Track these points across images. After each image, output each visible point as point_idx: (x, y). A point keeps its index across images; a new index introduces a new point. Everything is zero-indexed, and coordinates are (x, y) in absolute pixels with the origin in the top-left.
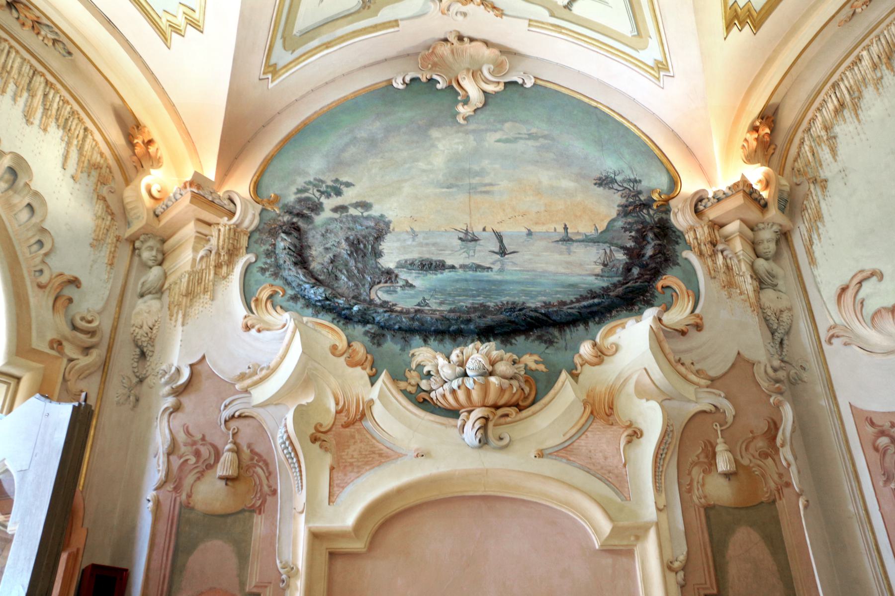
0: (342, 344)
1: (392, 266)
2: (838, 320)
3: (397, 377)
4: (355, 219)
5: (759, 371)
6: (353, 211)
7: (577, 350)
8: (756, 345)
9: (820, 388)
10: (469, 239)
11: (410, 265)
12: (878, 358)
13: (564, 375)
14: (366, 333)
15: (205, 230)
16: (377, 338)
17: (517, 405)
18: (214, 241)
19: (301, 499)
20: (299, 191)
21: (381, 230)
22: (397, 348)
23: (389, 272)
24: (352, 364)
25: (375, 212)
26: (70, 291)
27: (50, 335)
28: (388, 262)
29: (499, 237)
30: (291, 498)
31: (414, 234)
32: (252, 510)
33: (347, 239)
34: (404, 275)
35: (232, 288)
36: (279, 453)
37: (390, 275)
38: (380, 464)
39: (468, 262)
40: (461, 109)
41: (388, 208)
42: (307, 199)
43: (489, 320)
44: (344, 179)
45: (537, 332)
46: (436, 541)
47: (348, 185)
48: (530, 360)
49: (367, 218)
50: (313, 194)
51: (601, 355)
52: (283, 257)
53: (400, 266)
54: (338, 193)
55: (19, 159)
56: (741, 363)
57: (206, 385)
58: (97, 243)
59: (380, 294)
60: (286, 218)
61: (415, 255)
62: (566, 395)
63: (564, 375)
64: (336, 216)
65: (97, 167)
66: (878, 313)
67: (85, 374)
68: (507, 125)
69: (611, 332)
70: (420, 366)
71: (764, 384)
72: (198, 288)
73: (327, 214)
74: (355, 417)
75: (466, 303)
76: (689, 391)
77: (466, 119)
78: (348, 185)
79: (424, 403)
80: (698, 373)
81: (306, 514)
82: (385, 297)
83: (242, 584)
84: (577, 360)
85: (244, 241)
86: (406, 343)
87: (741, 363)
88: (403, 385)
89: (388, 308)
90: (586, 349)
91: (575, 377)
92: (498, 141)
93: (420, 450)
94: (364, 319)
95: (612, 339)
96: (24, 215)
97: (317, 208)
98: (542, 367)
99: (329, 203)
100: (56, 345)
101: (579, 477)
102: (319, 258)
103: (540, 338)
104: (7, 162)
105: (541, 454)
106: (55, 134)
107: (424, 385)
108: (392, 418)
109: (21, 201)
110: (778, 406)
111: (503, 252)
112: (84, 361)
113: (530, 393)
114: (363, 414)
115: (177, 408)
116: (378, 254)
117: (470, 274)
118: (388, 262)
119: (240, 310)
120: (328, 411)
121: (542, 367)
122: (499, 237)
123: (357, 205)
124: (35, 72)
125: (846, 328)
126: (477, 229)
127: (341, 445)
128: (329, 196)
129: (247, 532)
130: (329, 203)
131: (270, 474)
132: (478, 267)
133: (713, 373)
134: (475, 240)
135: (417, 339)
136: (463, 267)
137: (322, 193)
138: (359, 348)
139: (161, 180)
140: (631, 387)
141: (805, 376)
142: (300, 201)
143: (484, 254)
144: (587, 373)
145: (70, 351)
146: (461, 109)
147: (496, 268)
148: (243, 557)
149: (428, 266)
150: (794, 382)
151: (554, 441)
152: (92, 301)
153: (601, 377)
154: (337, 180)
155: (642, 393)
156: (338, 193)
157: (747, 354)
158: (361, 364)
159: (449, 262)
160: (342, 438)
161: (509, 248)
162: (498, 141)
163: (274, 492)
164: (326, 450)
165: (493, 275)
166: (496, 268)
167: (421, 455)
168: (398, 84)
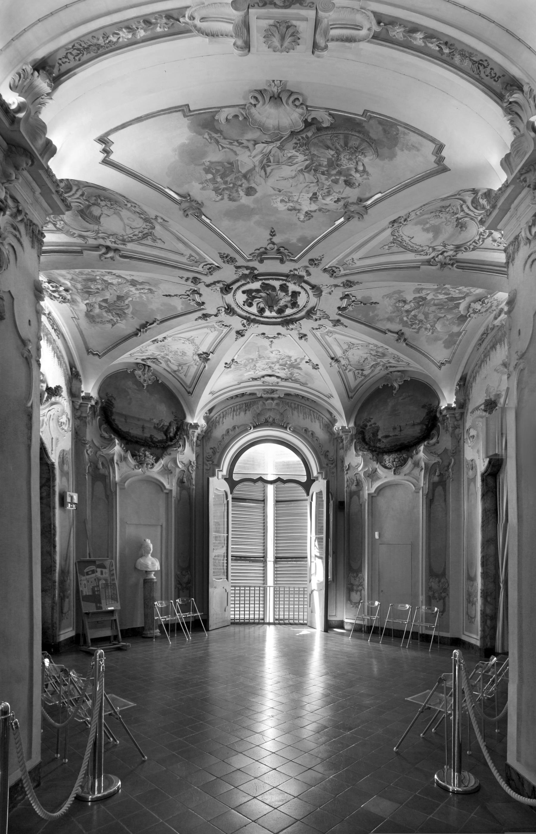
0: (372, 457)
6: (373, 426)
10: (395, 428)
16: (378, 454)
25: (377, 425)
26: (327, 454)
27: (326, 463)
28: (379, 437)
29: (400, 427)
35: (353, 448)
37: (380, 440)
41: (380, 424)
43: (397, 447)
46: (388, 493)
53: (382, 437)
54: (370, 421)
55: (312, 431)
57: (351, 468)
58: (330, 441)
59: (378, 445)
61: (384, 434)
62: (410, 463)
65: (326, 425)
67: (333, 468)
68: (404, 394)
72: (347, 449)
73: (368, 427)
74: (375, 471)
75: (393, 444)
81: (369, 489)
85: (354, 437)
86: (383, 455)
89: (379, 448)
93: (385, 476)
94: (375, 451)
96: (316, 442)
97: (366, 426)
99: (369, 424)
100: (327, 465)
101: (411, 479)
102: (367, 437)
104: (311, 432)
105: (405, 475)
106: (317, 421)
108: (381, 471)
109: (315, 439)
111: (401, 431)
112: (332, 466)
113: (403, 463)
115: (347, 473)
116: (377, 435)
118: (379, 437)
119: (355, 453)
122: (400, 427)
124: (310, 410)
127: (373, 477)
132: (396, 435)
135: (385, 454)
138: (374, 457)
139: (338, 426)
143: (397, 432)
145: (329, 465)
149: (387, 437)
151: (408, 472)
152: (331, 454)
153: (416, 457)
156: (370, 421)
165: (399, 437)
167: (386, 477)
168: (381, 387)
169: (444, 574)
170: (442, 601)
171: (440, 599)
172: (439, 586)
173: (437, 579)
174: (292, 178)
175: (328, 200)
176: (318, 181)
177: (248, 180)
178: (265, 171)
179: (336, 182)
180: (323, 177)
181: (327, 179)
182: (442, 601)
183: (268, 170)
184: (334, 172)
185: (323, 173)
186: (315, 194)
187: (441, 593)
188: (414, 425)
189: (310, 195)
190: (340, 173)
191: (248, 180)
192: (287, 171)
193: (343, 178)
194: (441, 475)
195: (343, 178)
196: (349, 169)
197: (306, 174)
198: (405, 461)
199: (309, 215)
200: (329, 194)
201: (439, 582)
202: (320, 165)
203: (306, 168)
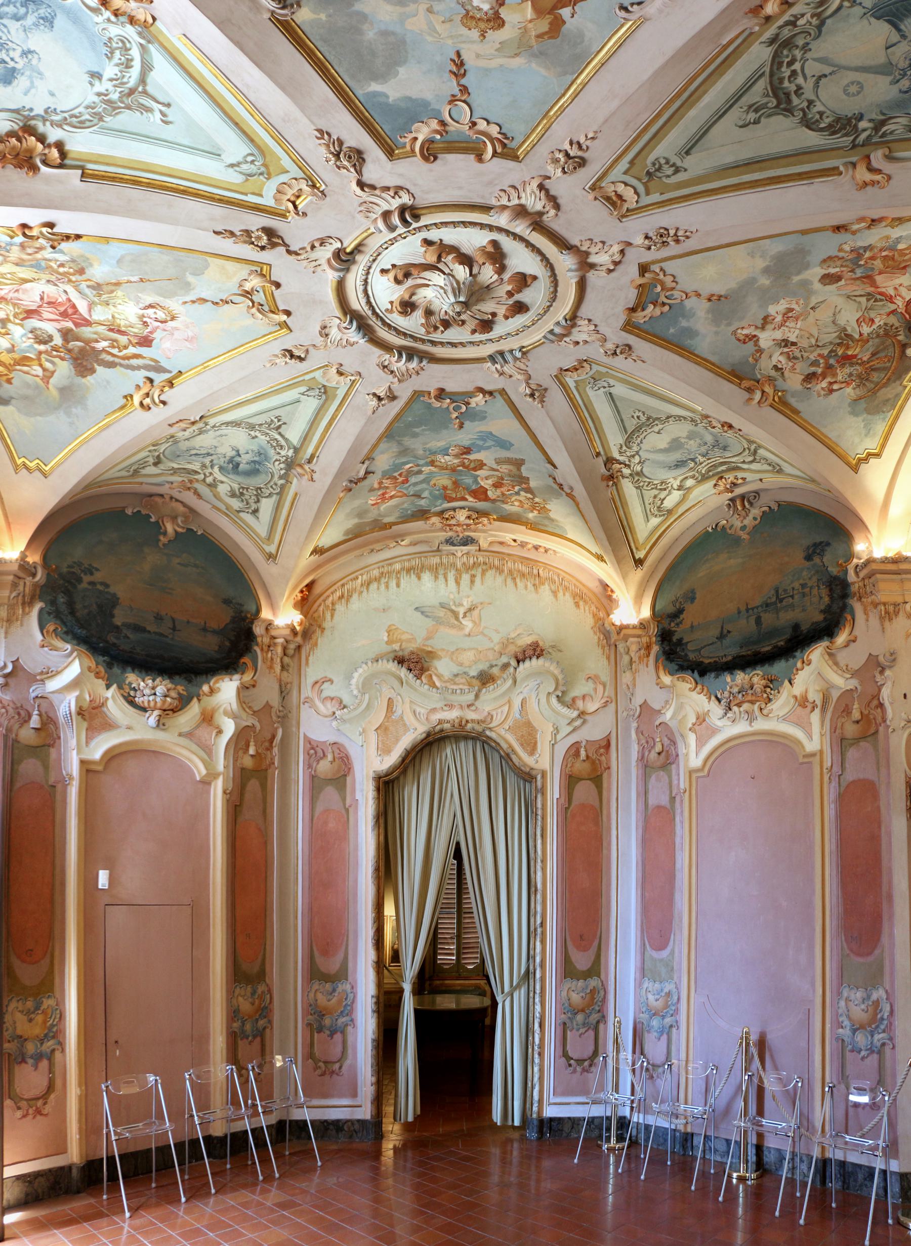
1: (119, 624)
2: (310, 695)
3: (120, 687)
4: (100, 592)
5: (273, 710)
7: (201, 687)
8: (275, 701)
9: (294, 722)
11: (127, 626)
12: (320, 717)
13: (195, 700)
14: (104, 661)
15: (16, 580)
17: (172, 710)
18: (21, 588)
19: (73, 743)
20: (69, 567)
21: (114, 601)
22: (119, 671)
23: (117, 627)
24: (97, 677)
30: (66, 742)
31: (131, 608)
32: (49, 746)
33: (96, 603)
34: (125, 631)
36: (61, 720)
38: (109, 730)
39: (157, 630)
40: (162, 538)
42: (74, 573)
44: (95, 566)
45: (184, 675)
47: (97, 570)
48: (180, 688)
49: (107, 593)
50: (76, 570)
51: (212, 691)
52: (63, 608)
56: (268, 706)
60: (61, 582)
63: (195, 700)
64: (90, 587)
66: (326, 698)
69: (217, 682)
70: (130, 684)
71: (274, 718)
76: (244, 715)
77: (164, 545)
78: (97, 570)
79: (132, 703)
80: (250, 707)
82: (115, 641)
83: (47, 781)
84: (201, 693)
87: (268, 706)
88: (122, 691)
90: (205, 688)
91: (199, 700)
92: (179, 564)
95: (217, 685)
98: (185, 693)
103: (185, 678)
107: (132, 693)
110: (277, 728)
114: (103, 704)
117: (157, 637)
120: (85, 700)
121: (185, 693)
123: (102, 584)
125: (312, 700)
126: (163, 613)
128: (86, 574)
129: (48, 755)
130: (86, 578)
131: (57, 728)
133: (256, 709)
134: (161, 619)
136: (155, 633)
137: (83, 571)
140: (221, 710)
141: (290, 715)
142: (69, 572)
144: (205, 699)
146: (162, 538)
147: (170, 636)
148: (46, 767)
150: (285, 717)
154: (90, 565)
155: (226, 713)
157: (271, 703)
158: (102, 678)
159: (148, 628)
160: (92, 716)
161: (178, 627)
162: (179, 564)
163: (59, 738)
164: (85, 720)
166: (170, 636)
169: (261, 975)
170: (258, 1039)
171: (255, 1037)
172: (253, 1004)
173: (249, 989)
182: (258, 1039)
187: (257, 1020)
188: (205, 630)
194: (257, 756)
198: (183, 702)
201: (253, 993)
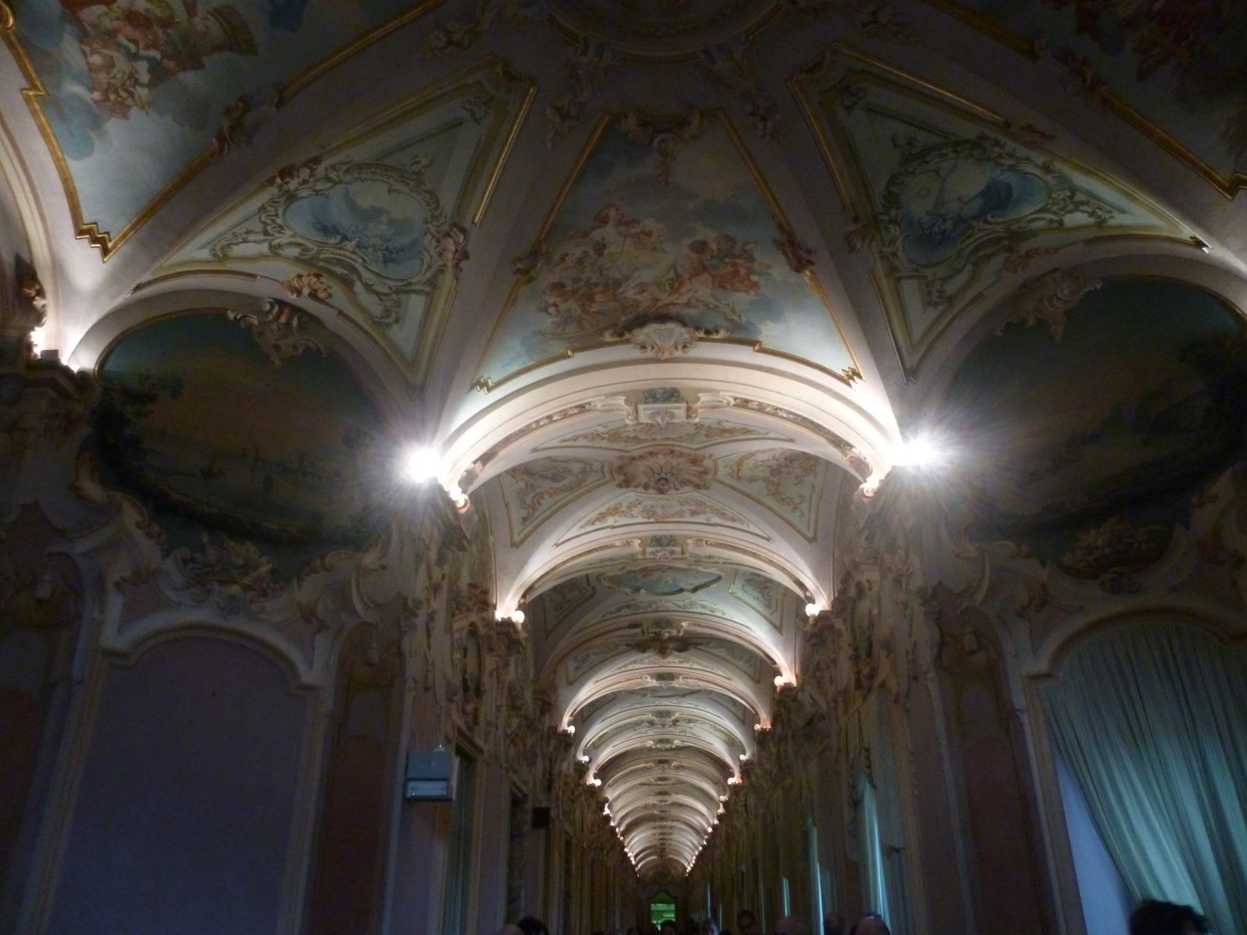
174: (637, 269)
175: (578, 253)
176: (601, 272)
177: (701, 263)
178: (676, 273)
179: (576, 280)
180: (594, 280)
181: (589, 279)
183: (671, 275)
184: (583, 291)
185: (596, 285)
186: (600, 254)
189: (606, 252)
190: (574, 292)
191: (701, 263)
192: (646, 276)
193: (569, 288)
195: (569, 288)
196: (566, 301)
197: (618, 276)
199: (602, 221)
200: (580, 262)
202: (603, 292)
203: (620, 286)
